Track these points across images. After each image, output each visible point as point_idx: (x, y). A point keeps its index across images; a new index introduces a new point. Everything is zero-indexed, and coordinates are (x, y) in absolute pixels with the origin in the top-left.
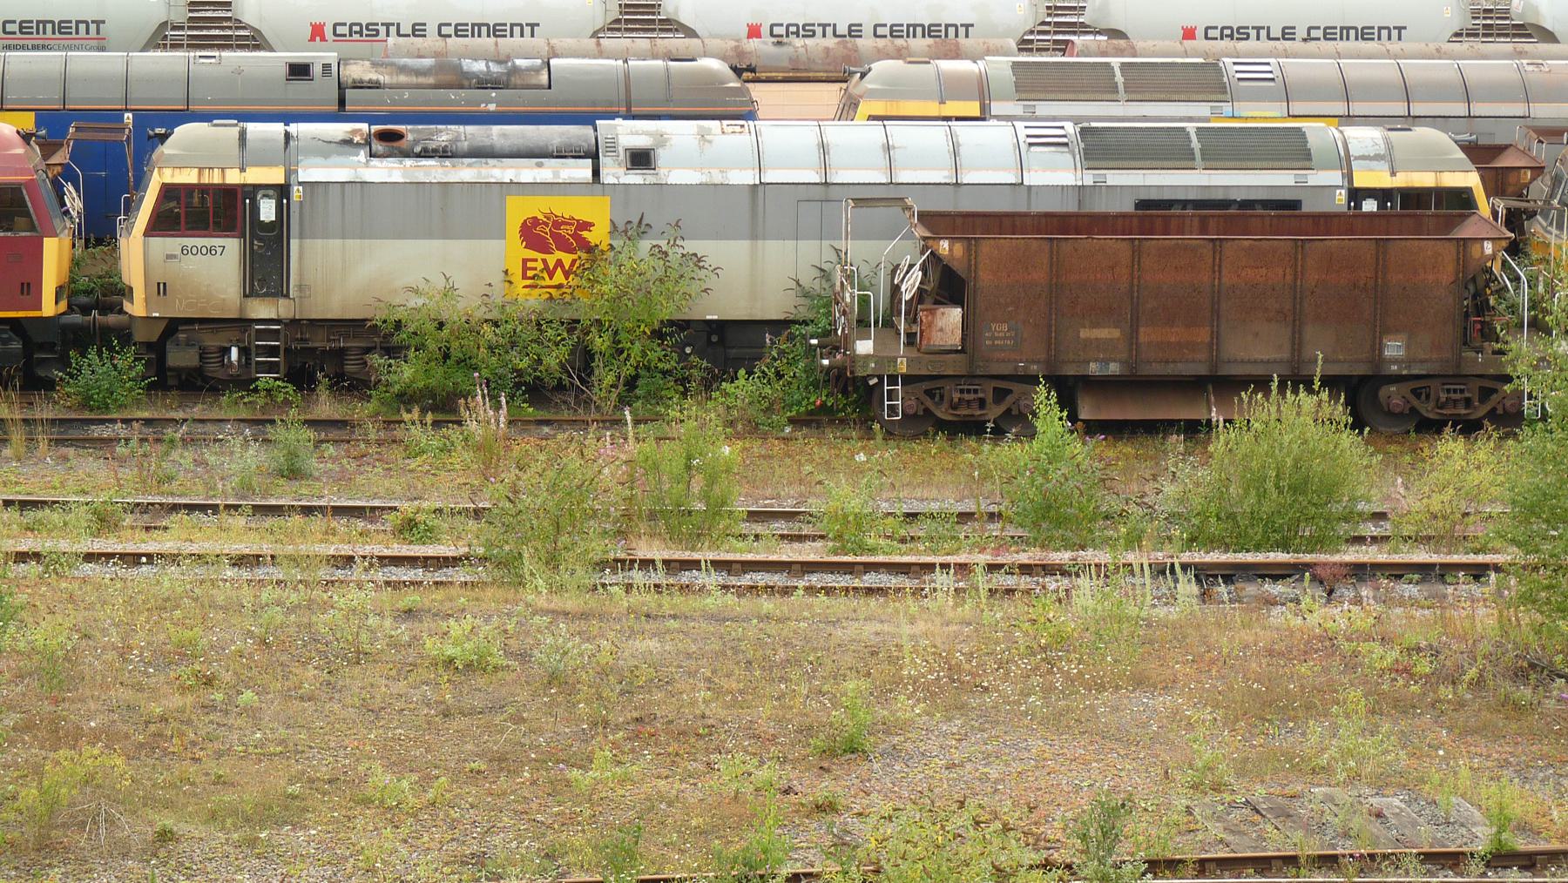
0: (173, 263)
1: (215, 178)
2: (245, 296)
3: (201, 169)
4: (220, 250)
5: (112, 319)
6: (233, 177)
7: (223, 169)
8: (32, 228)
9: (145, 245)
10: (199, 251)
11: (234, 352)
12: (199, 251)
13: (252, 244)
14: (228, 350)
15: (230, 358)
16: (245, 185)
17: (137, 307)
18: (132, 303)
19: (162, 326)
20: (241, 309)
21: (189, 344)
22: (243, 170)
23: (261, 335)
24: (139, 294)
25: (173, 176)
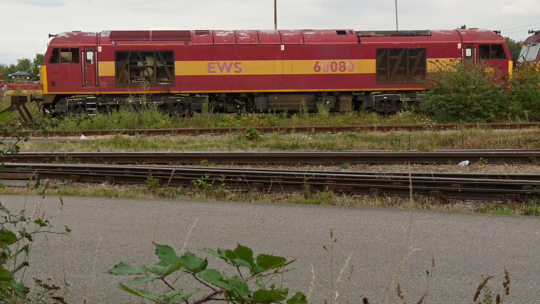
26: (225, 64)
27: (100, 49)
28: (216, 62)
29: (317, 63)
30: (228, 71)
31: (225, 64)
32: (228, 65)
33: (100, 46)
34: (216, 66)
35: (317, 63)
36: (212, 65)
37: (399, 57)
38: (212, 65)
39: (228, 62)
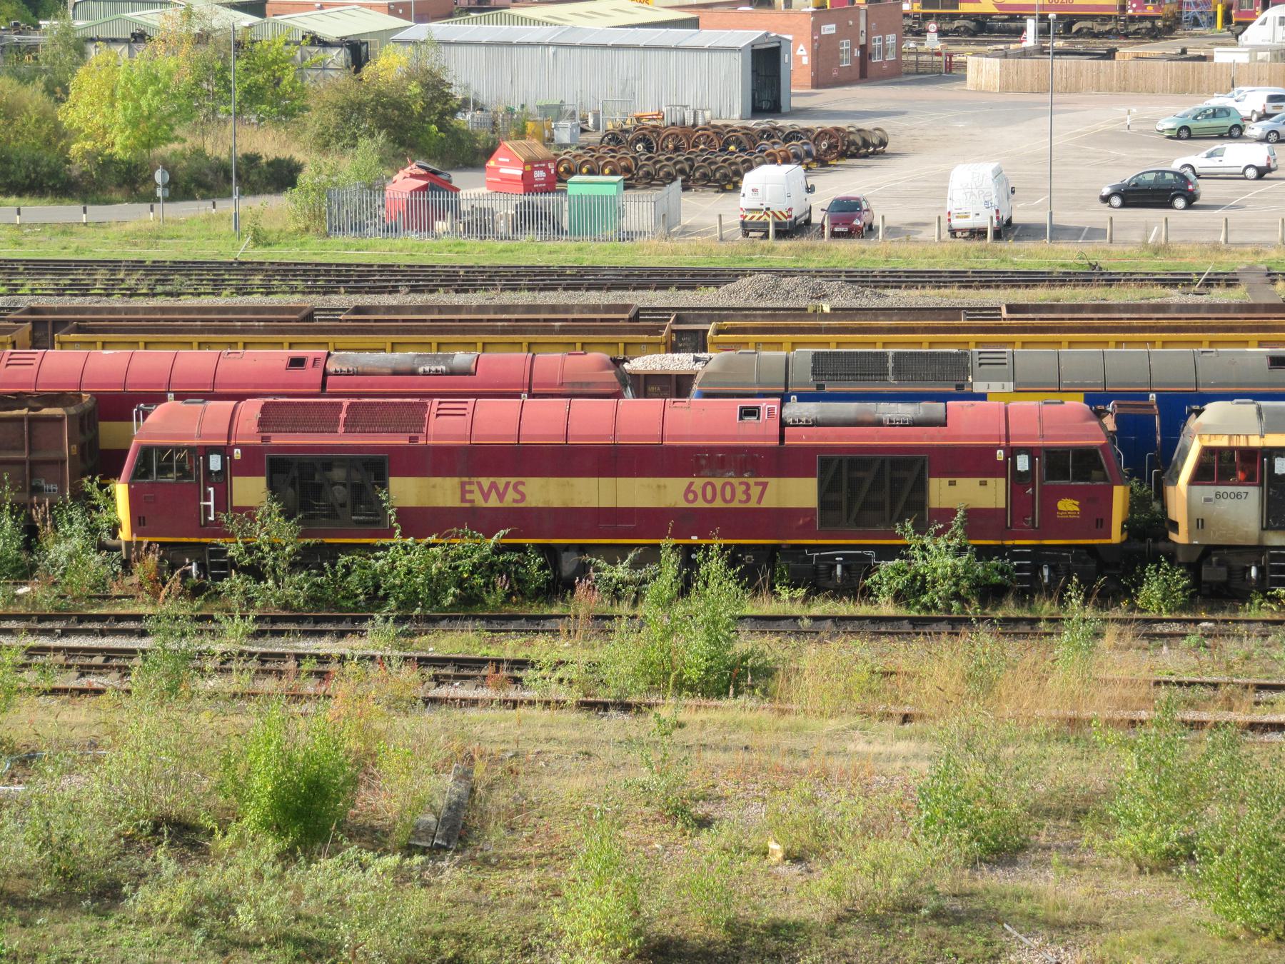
1: (1242, 443)
2: (1263, 529)
3: (1230, 436)
4: (1244, 495)
5: (1161, 545)
6: (1255, 442)
7: (1247, 436)
8: (1105, 479)
9: (1189, 492)
10: (1229, 495)
11: (1254, 572)
12: (1229, 495)
13: (1268, 491)
14: (1250, 569)
17: (1181, 537)
18: (1178, 533)
19: (1200, 551)
20: (1260, 538)
21: (1219, 564)
22: (1262, 436)
23: (1274, 558)
24: (1183, 527)
25: (1210, 440)
26: (494, 486)
27: (237, 453)
28: (475, 479)
29: (691, 484)
30: (501, 499)
31: (493, 486)
32: (501, 488)
34: (475, 488)
35: (691, 484)
37: (868, 476)
38: (468, 487)
39: (501, 481)
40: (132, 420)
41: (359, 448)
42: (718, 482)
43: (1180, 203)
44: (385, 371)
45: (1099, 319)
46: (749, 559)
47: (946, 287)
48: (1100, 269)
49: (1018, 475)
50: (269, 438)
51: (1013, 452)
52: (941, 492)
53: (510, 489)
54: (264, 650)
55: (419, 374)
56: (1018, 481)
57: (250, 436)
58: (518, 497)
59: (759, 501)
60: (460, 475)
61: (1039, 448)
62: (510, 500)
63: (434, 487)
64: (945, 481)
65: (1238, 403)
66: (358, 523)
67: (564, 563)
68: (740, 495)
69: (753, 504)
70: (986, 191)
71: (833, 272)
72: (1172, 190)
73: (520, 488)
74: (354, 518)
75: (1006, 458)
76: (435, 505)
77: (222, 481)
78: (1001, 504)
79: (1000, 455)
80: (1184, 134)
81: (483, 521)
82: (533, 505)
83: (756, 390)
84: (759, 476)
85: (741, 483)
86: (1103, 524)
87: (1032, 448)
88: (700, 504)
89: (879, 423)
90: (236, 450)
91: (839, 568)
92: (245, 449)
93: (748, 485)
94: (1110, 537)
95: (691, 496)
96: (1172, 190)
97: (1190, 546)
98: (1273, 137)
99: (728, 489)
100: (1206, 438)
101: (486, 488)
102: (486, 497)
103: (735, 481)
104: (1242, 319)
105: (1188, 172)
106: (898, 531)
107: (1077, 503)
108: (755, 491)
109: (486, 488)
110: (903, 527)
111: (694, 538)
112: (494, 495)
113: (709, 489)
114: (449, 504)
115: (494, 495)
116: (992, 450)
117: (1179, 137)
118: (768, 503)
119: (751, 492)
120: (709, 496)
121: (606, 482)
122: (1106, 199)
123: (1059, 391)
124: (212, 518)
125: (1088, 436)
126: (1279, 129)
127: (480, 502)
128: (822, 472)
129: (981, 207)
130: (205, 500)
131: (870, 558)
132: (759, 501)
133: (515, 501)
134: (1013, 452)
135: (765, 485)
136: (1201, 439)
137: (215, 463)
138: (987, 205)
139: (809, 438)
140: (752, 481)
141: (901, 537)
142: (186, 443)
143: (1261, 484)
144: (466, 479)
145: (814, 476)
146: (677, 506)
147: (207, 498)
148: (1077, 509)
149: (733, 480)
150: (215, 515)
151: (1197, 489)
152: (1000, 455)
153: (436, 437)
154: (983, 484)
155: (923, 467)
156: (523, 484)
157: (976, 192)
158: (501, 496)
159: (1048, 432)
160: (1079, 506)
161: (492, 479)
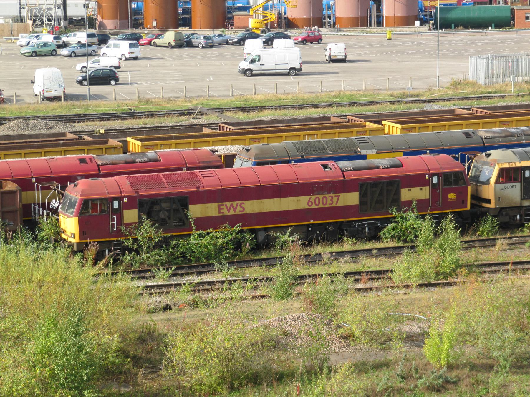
0: (502, 192)
1: (514, 166)
2: (522, 199)
3: (509, 163)
6: (518, 165)
7: (515, 163)
9: (495, 187)
11: (518, 217)
14: (517, 216)
15: (517, 218)
16: (522, 167)
19: (499, 210)
20: (521, 203)
21: (506, 215)
22: (520, 162)
24: (493, 201)
25: (502, 165)
26: (232, 205)
27: (125, 200)
28: (224, 203)
29: (310, 198)
32: (235, 206)
33: (125, 197)
34: (224, 207)
35: (310, 198)
36: (221, 207)
38: (221, 207)
39: (235, 203)
40: (34, 190)
41: (176, 194)
42: (321, 197)
43: (113, 82)
44: (122, 162)
45: (315, 124)
46: (331, 228)
47: (93, 121)
48: (135, 111)
49: (434, 185)
50: (138, 192)
51: (432, 175)
52: (406, 194)
53: (239, 206)
54: (176, 282)
55: (136, 162)
56: (434, 188)
57: (130, 192)
58: (242, 209)
59: (337, 204)
60: (218, 202)
61: (441, 173)
62: (238, 211)
63: (207, 208)
64: (407, 189)
65: (503, 150)
66: (176, 226)
67: (259, 236)
68: (329, 202)
69: (334, 205)
70: (59, 80)
71: (54, 116)
72: (109, 77)
73: (243, 205)
74: (174, 224)
75: (429, 178)
76: (208, 216)
77: (118, 212)
78: (428, 197)
79: (427, 177)
80: (34, 54)
81: (233, 220)
82: (248, 212)
83: (278, 159)
84: (336, 193)
85: (329, 197)
86: (464, 202)
87: (439, 173)
88: (314, 206)
89: (377, 168)
90: (125, 199)
91: (367, 229)
92: (128, 197)
93: (332, 197)
94: (466, 207)
95: (310, 204)
96: (109, 77)
97: (496, 208)
98: (73, 54)
99: (325, 199)
100: (500, 164)
101: (229, 207)
102: (229, 210)
103: (327, 196)
104: (314, 125)
105: (112, 68)
106: (390, 211)
107: (455, 194)
108: (335, 199)
109: (229, 207)
110: (392, 210)
111: (312, 221)
112: (232, 210)
113: (317, 200)
114: (214, 215)
115: (232, 210)
116: (424, 175)
117: (32, 56)
118: (340, 204)
119: (333, 200)
120: (317, 203)
121: (277, 200)
122: (80, 82)
123: (393, 152)
124: (115, 229)
125: (458, 167)
126: (75, 51)
127: (226, 213)
128: (360, 190)
129: (57, 87)
130: (112, 222)
131: (377, 224)
132: (337, 204)
133: (240, 211)
134: (432, 175)
135: (339, 197)
136: (498, 165)
137: (116, 205)
138: (60, 86)
139: (355, 176)
140: (333, 195)
141: (392, 214)
142: (103, 197)
143: (521, 182)
144: (221, 203)
145: (357, 191)
146: (305, 208)
147: (113, 221)
148: (455, 197)
149: (326, 196)
150: (117, 228)
151: (498, 185)
152: (427, 177)
153: (207, 186)
154: (421, 189)
155: (398, 185)
156: (243, 203)
157: (54, 80)
158: (235, 210)
159: (443, 166)
160: (456, 196)
161: (231, 203)
